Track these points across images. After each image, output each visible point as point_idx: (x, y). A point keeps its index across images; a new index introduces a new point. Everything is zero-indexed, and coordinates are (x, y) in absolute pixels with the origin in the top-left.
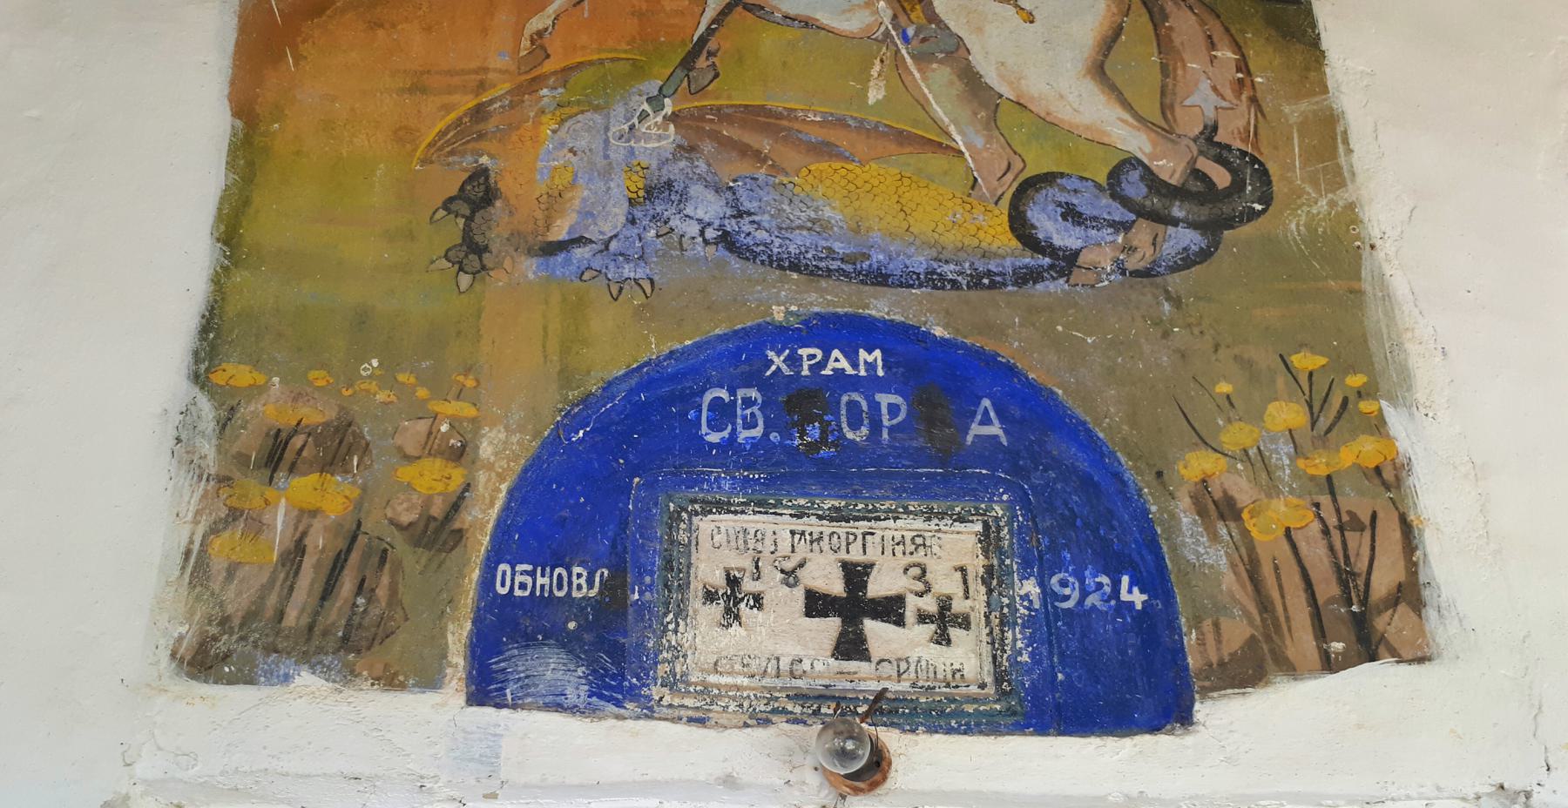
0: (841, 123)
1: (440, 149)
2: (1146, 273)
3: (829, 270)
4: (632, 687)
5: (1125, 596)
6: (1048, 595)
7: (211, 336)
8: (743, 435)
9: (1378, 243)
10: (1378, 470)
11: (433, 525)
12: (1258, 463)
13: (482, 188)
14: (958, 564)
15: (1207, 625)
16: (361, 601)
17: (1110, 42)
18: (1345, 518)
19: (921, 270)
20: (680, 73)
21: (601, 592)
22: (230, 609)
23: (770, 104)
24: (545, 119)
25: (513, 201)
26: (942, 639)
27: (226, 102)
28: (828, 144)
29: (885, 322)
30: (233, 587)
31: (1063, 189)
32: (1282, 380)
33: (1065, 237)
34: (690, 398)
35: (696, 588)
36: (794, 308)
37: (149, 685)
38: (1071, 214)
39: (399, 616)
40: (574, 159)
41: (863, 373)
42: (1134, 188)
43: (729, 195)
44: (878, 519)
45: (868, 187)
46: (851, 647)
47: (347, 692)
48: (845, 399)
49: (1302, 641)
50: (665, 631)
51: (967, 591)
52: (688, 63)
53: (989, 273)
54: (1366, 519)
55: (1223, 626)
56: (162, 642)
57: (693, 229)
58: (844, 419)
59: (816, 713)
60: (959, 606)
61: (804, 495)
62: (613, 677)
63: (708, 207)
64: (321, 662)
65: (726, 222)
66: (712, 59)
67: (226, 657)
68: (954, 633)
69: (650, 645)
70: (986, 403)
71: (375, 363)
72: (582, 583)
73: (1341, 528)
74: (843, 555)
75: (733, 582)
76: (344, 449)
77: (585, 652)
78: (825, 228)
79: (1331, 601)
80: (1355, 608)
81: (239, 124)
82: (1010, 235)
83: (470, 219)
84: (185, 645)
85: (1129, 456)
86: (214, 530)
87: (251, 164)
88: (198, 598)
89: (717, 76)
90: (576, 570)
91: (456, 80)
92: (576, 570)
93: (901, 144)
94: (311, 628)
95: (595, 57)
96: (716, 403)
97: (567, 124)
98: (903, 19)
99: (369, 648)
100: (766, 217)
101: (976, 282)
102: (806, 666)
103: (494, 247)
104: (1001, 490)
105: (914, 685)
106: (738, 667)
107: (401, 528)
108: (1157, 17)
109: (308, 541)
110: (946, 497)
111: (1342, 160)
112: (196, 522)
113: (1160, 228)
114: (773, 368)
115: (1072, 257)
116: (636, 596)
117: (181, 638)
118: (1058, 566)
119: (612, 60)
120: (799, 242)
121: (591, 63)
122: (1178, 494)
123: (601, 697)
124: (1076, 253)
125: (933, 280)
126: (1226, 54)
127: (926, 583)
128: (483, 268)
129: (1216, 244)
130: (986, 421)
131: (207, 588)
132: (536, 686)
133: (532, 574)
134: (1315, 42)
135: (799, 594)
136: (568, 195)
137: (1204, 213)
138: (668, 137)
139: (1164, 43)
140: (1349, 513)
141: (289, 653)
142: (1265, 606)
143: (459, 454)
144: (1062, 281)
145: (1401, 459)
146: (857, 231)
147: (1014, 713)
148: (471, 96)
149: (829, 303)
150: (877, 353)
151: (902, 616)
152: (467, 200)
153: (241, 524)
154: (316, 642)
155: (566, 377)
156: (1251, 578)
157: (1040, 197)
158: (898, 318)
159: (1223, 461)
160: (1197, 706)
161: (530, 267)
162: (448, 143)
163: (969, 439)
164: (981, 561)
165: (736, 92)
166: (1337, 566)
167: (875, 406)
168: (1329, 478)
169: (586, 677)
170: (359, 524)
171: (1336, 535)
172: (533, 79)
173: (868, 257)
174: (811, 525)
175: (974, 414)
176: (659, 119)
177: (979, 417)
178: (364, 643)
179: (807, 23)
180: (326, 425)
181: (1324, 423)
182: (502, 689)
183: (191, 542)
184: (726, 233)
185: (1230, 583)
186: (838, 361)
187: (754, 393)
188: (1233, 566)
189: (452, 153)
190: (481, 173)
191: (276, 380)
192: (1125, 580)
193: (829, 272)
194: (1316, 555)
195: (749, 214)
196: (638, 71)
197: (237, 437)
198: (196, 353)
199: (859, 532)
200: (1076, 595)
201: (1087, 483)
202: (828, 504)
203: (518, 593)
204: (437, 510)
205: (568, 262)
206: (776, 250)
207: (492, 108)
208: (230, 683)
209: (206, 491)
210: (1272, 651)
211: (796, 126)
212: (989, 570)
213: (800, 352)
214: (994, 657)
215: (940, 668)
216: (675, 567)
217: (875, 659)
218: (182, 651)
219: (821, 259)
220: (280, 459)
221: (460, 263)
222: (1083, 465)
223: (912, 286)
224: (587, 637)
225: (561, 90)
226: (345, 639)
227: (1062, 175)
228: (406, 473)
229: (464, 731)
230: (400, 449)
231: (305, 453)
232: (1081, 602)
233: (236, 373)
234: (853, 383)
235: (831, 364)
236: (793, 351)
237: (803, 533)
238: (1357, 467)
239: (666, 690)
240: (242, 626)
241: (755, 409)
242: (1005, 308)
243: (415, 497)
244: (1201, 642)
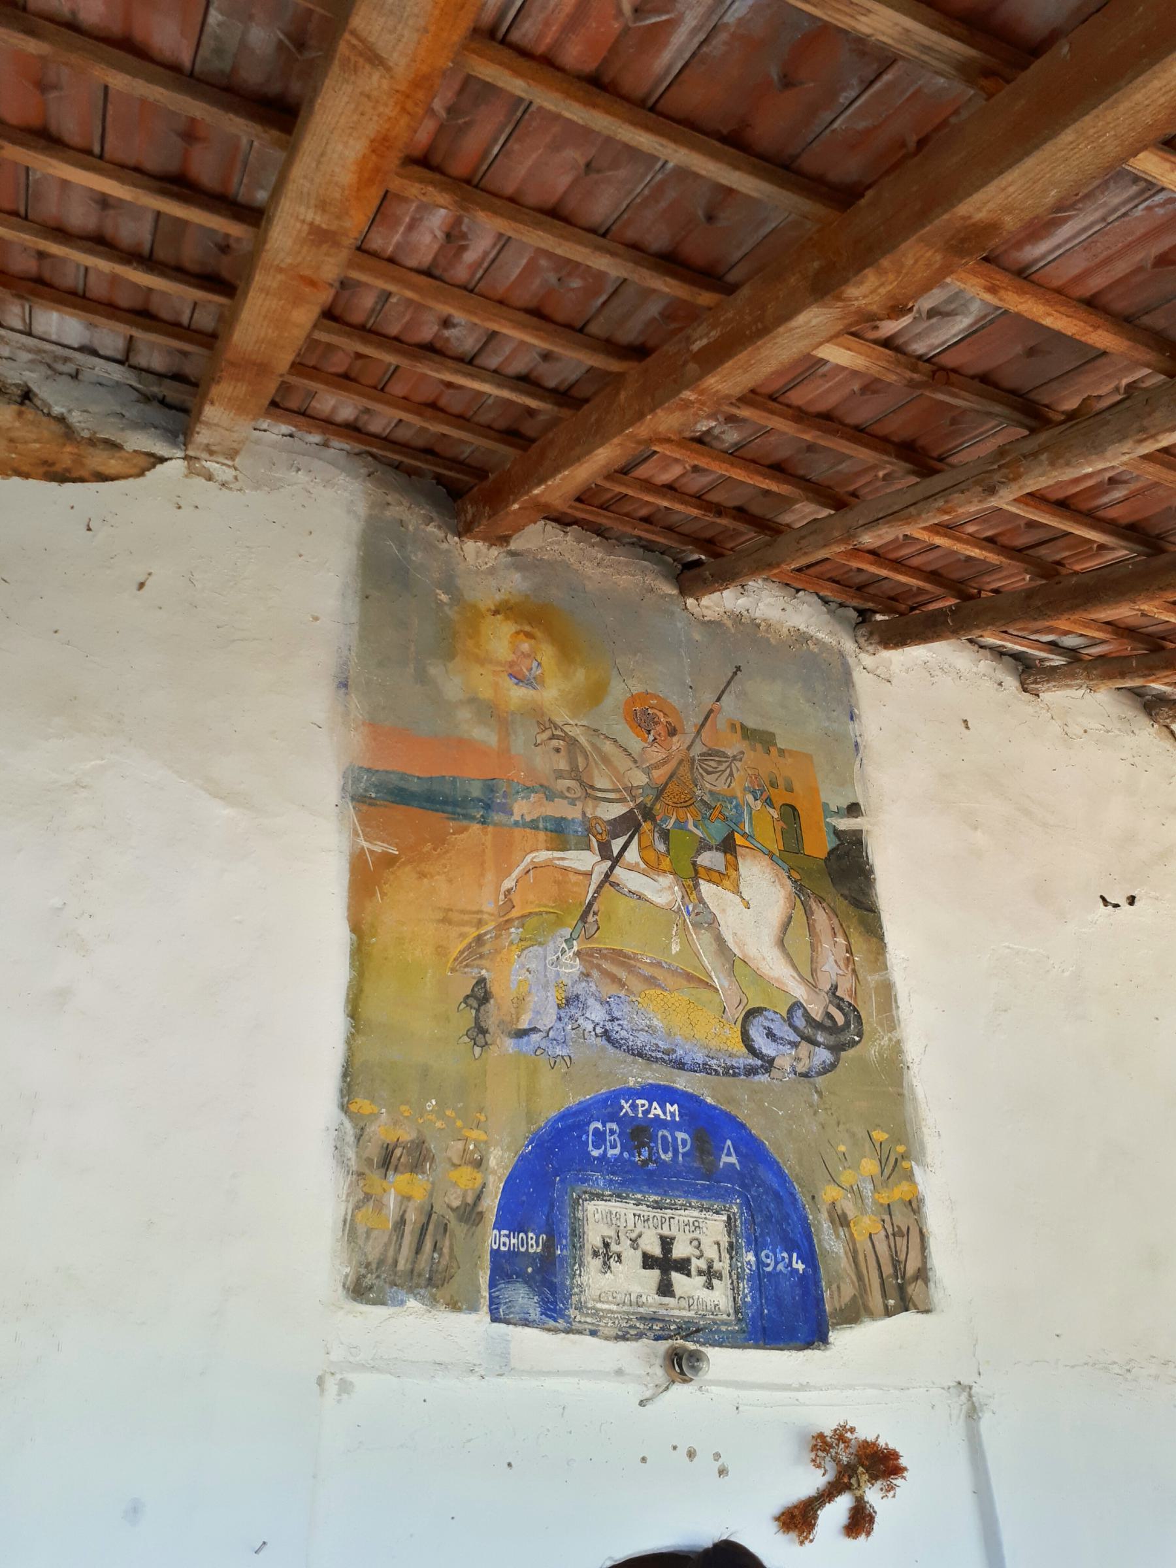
0: (659, 964)
1: (461, 962)
2: (805, 1075)
3: (657, 1058)
4: (561, 1309)
5: (795, 1266)
6: (759, 1262)
7: (348, 1079)
8: (611, 1153)
9: (911, 1065)
10: (910, 1202)
11: (468, 1209)
12: (858, 1195)
13: (483, 990)
14: (715, 1239)
15: (834, 1286)
16: (436, 1255)
17: (786, 925)
18: (896, 1229)
19: (700, 1062)
20: (580, 925)
21: (543, 1249)
22: (370, 1258)
23: (626, 949)
24: (514, 947)
25: (499, 1001)
26: (709, 1286)
27: (347, 922)
28: (654, 978)
29: (682, 1091)
30: (370, 1243)
31: (766, 1018)
32: (868, 1144)
33: (768, 1048)
34: (582, 1127)
35: (588, 1248)
36: (639, 1080)
37: (333, 1304)
38: (770, 1034)
39: (455, 1265)
40: (530, 976)
41: (669, 1118)
42: (800, 1022)
43: (607, 1006)
44: (676, 1209)
45: (674, 1007)
46: (665, 1289)
47: (434, 1312)
48: (660, 1134)
49: (875, 1299)
50: (575, 1275)
51: (720, 1257)
52: (583, 918)
53: (732, 1067)
54: (905, 1230)
55: (842, 1288)
56: (338, 1277)
57: (590, 1027)
58: (660, 1146)
59: (651, 1329)
60: (717, 1266)
61: (640, 1192)
62: (552, 1303)
63: (597, 1013)
64: (419, 1293)
65: (606, 1023)
66: (596, 917)
67: (370, 1288)
68: (715, 1282)
69: (568, 1283)
70: (729, 1142)
71: (434, 1102)
72: (533, 1243)
73: (894, 1235)
74: (659, 1231)
75: (606, 1245)
76: (422, 1158)
77: (537, 1287)
78: (654, 1032)
79: (888, 1277)
80: (899, 1281)
81: (354, 937)
82: (742, 1044)
83: (478, 1010)
84: (349, 1278)
85: (799, 1184)
86: (357, 1207)
87: (362, 965)
88: (353, 1250)
89: (598, 929)
90: (531, 1235)
91: (466, 917)
92: (531, 1235)
93: (689, 981)
94: (412, 1271)
95: (537, 910)
96: (596, 1129)
97: (525, 952)
98: (686, 899)
99: (442, 1285)
100: (625, 1022)
101: (726, 1074)
102: (644, 1299)
103: (491, 1030)
104: (738, 1201)
105: (696, 1313)
106: (610, 1299)
107: (453, 1210)
108: (809, 913)
109: (407, 1216)
110: (710, 1198)
111: (894, 1012)
112: (348, 1201)
113: (812, 1047)
114: (624, 1111)
115: (771, 1061)
116: (559, 1252)
117: (347, 1276)
118: (764, 1247)
119: (547, 913)
120: (641, 1039)
121: (536, 914)
122: (822, 1210)
123: (547, 1316)
124: (773, 1059)
125: (706, 1069)
126: (841, 940)
127: (701, 1251)
128: (486, 1044)
129: (837, 1060)
130: (729, 1154)
131: (356, 1243)
132: (514, 1307)
133: (508, 1236)
134: (881, 938)
135: (639, 1254)
136: (527, 999)
137: (832, 1040)
138: (575, 967)
139: (811, 927)
140: (898, 1226)
141: (402, 1287)
142: (860, 1278)
143: (479, 1164)
144: (767, 1075)
145: (920, 1196)
146: (669, 1034)
147: (744, 1332)
148: (474, 929)
149: (657, 1078)
150: (676, 1106)
151: (689, 1271)
152: (476, 998)
153: (371, 1203)
154: (415, 1280)
155: (530, 1117)
156: (854, 1262)
157: (755, 1022)
158: (690, 1090)
159: (842, 1191)
160: (830, 1334)
161: (509, 1045)
162: (465, 959)
163: (721, 1164)
164: (726, 1239)
165: (608, 941)
166: (892, 1256)
167: (675, 1139)
168: (889, 1205)
169: (538, 1303)
170: (432, 1207)
171: (891, 1237)
172: (507, 921)
173: (675, 1052)
174: (644, 1210)
175: (723, 1148)
176: (571, 954)
177: (725, 1151)
178: (440, 1282)
179: (640, 897)
180: (412, 1142)
181: (887, 1172)
182: (497, 1309)
183: (346, 1214)
184: (606, 1031)
185: (845, 1263)
186: (656, 1110)
187: (614, 1126)
188: (846, 1253)
189: (467, 966)
190: (482, 981)
191: (384, 1110)
192: (795, 1255)
193: (657, 1060)
194: (882, 1248)
195: (618, 1020)
196: (559, 922)
197: (366, 1147)
198: (341, 1091)
199: (667, 1217)
200: (773, 1264)
201: (777, 1195)
202: (653, 1198)
203: (502, 1248)
204: (470, 1200)
205: (528, 1044)
206: (631, 1043)
207: (486, 938)
208: (374, 1304)
209: (351, 1181)
210: (863, 1304)
211: (638, 965)
212: (731, 1244)
213: (637, 1101)
214: (734, 1298)
215: (708, 1305)
216: (577, 1233)
217: (677, 1297)
218: (348, 1283)
219: (653, 1051)
220: (390, 1162)
221: (474, 1039)
222: (776, 1186)
223: (696, 1071)
224: (538, 1277)
225: (521, 930)
226: (430, 1279)
227: (766, 1009)
228: (454, 1175)
229: (492, 1338)
230: (450, 1159)
231: (402, 1160)
232: (775, 1268)
233: (363, 1105)
234: (662, 1124)
235: (653, 1111)
236: (634, 1101)
237: (639, 1216)
238: (902, 1200)
239: (577, 1312)
240: (377, 1269)
241: (615, 1136)
242: (740, 1088)
243: (459, 1190)
244: (832, 1298)
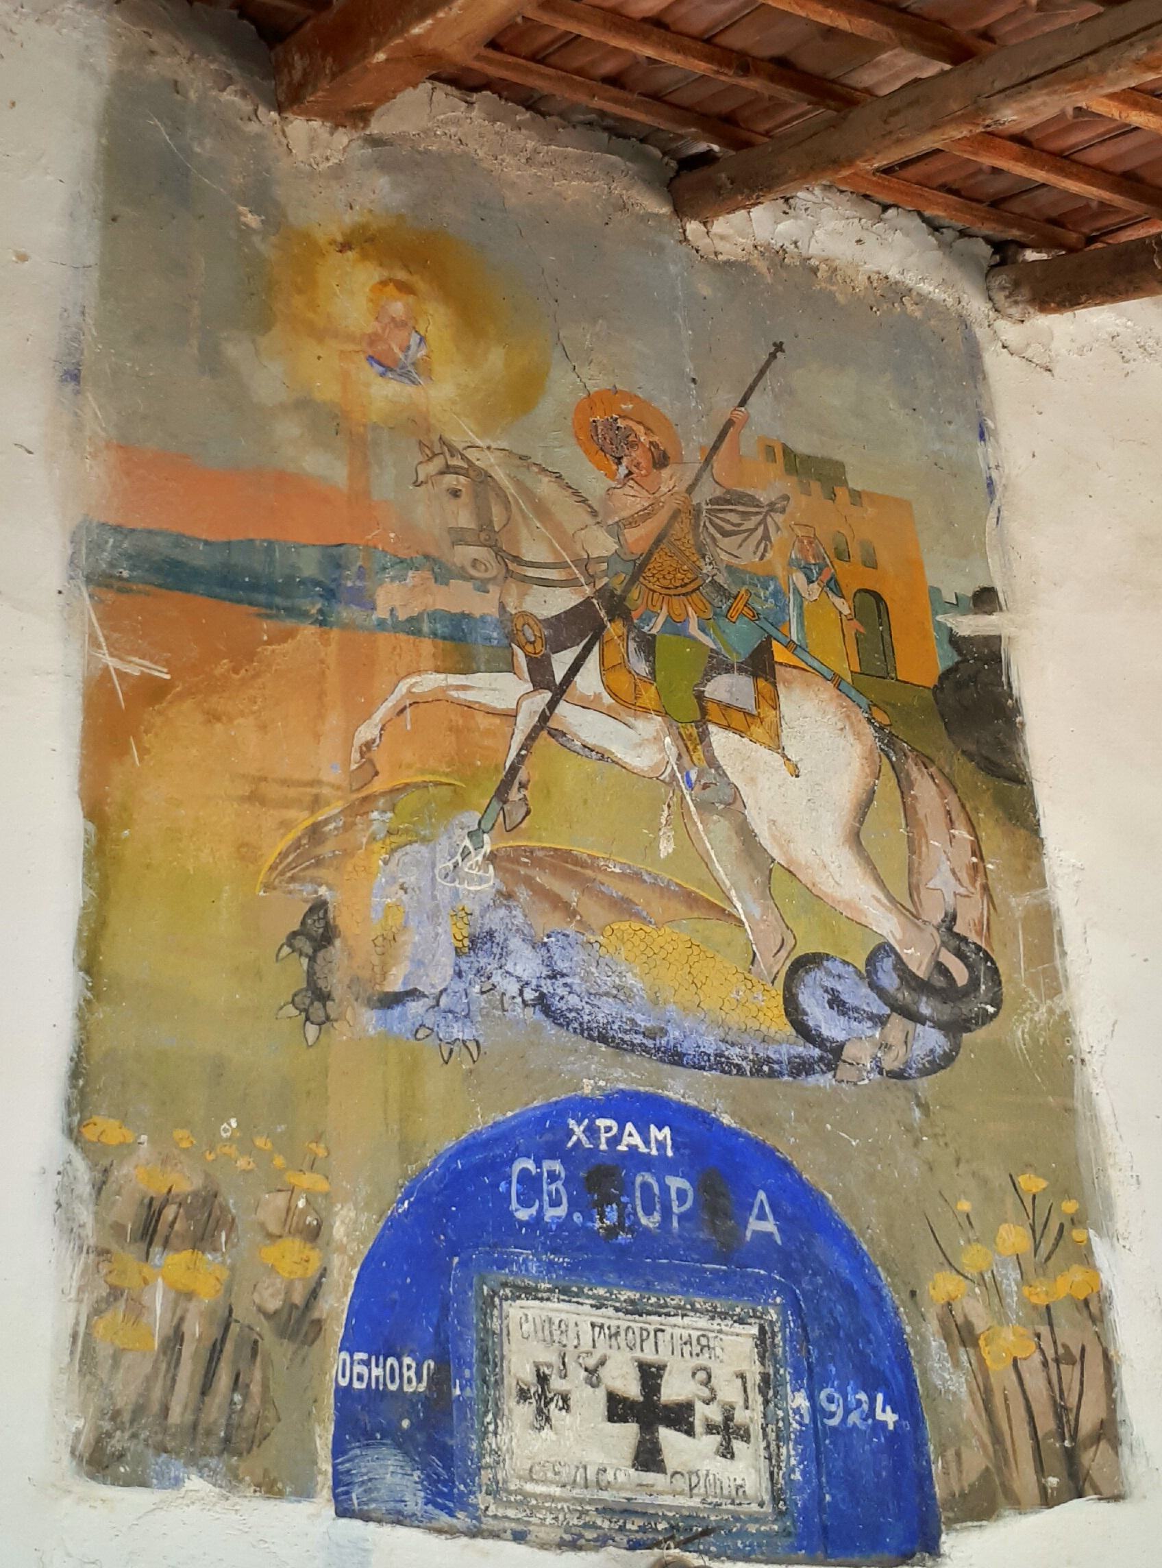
0: (636, 877)
1: (282, 873)
2: (899, 1075)
3: (633, 1044)
4: (461, 1493)
5: (880, 1416)
6: (815, 1409)
7: (81, 1082)
8: (551, 1214)
9: (1087, 1057)
10: (1086, 1302)
11: (295, 1314)
12: (991, 1287)
13: (322, 923)
15: (950, 1453)
16: (237, 1398)
17: (864, 806)
18: (1061, 1351)
19: (710, 1051)
20: (496, 805)
21: (429, 1387)
22: (120, 1403)
23: (580, 850)
24: (377, 846)
26: (727, 1452)
27: (78, 801)
29: (678, 1103)
31: (829, 973)
32: (1010, 1199)
33: (832, 1027)
34: (499, 1168)
35: (510, 1383)
36: (602, 1083)
37: (54, 1485)
38: (836, 1002)
39: (271, 1414)
40: (405, 897)
41: (654, 1152)
42: (890, 981)
43: (543, 951)
44: (668, 1315)
45: (663, 954)
47: (234, 1499)
48: (639, 1180)
49: (1024, 1476)
50: (486, 1433)
51: (746, 1400)
52: (501, 793)
53: (768, 1061)
54: (1076, 1352)
55: (964, 1456)
56: (62, 1437)
57: (513, 988)
58: (638, 1202)
59: (622, 1529)
60: (740, 1416)
61: (604, 1284)
62: (445, 1483)
64: (206, 1466)
65: (543, 982)
66: (523, 792)
67: (120, 1457)
68: (737, 1445)
69: (474, 1447)
70: (762, 1195)
71: (234, 1123)
73: (1057, 1361)
74: (638, 1354)
75: (543, 1379)
77: (419, 1454)
79: (1047, 1436)
80: (1067, 1443)
81: (91, 827)
82: (785, 1020)
83: (312, 959)
84: (83, 1439)
85: (888, 1271)
86: (97, 1312)
87: (105, 877)
88: (89, 1389)
89: (528, 813)
90: (407, 1360)
91: (292, 792)
92: (407, 1360)
94: (195, 1426)
95: (419, 779)
96: (524, 1171)
97: (397, 855)
98: (686, 758)
99: (249, 1451)
100: (577, 980)
101: (757, 1072)
102: (609, 1476)
103: (335, 995)
104: (778, 1300)
105: (704, 1501)
106: (550, 1475)
107: (269, 1316)
108: (904, 785)
109: (186, 1327)
110: (728, 1294)
111: (1058, 962)
112: (80, 1301)
113: (910, 1025)
114: (574, 1138)
115: (838, 1049)
116: (457, 1392)
117: (78, 1434)
118: (825, 1382)
119: (438, 784)
120: (605, 1011)
121: (417, 786)
122: (928, 1316)
125: (721, 1064)
126: (962, 833)
127: (712, 1390)
128: (328, 1018)
129: (956, 1048)
130: (762, 1217)
131: (94, 1375)
132: (378, 1490)
133: (367, 1363)
135: (601, 1395)
137: (946, 1012)
138: (487, 881)
139: (909, 811)
140: (1064, 1346)
141: (177, 1454)
142: (997, 1437)
143: (314, 1234)
144: (830, 1075)
145: (1104, 1292)
146: (655, 1002)
149: (633, 1081)
150: (667, 1130)
151: (691, 1425)
152: (310, 938)
153: (122, 1304)
154: (201, 1442)
155: (406, 1150)
156: (986, 1409)
157: (809, 979)
158: (692, 1102)
160: (943, 1538)
161: (369, 1020)
162: (289, 867)
163: (748, 1234)
166: (1055, 1401)
167: (665, 1189)
168: (1048, 1308)
169: (421, 1483)
171: (1052, 1365)
172: (365, 799)
173: (664, 1032)
174: (609, 1317)
175: (752, 1206)
176: (480, 858)
177: (755, 1211)
178: (244, 1445)
180: (195, 1194)
181: (1045, 1249)
182: (347, 1493)
183: (77, 1324)
185: (969, 1412)
186: (632, 1138)
187: (557, 1166)
188: (971, 1393)
189: (293, 879)
190: (319, 907)
191: (144, 1138)
192: (880, 1397)
194: (1036, 1384)
195: (563, 975)
196: (458, 801)
197: (114, 1203)
199: (651, 1328)
200: (840, 1413)
201: (848, 1291)
202: (626, 1294)
203: (357, 1385)
204: (298, 1298)
205: (402, 1018)
206: (586, 1018)
207: (327, 829)
208: (127, 1484)
209: (86, 1264)
210: (1003, 1484)
211: (600, 877)
212: (765, 1378)
214: (772, 1474)
215: (725, 1485)
216: (490, 1358)
217: (670, 1471)
218: (80, 1447)
219: (626, 1032)
220: (155, 1231)
221: (306, 1011)
222: (846, 1273)
223: (703, 1068)
224: (420, 1437)
225: (390, 815)
226: (227, 1440)
227: (827, 957)
228: (270, 1253)
229: (338, 1545)
230: (262, 1226)
231: (177, 1226)
233: (107, 1129)
235: (626, 1140)
236: (592, 1122)
237: (602, 1327)
238: (1071, 1298)
239: (490, 1498)
240: (132, 1422)
241: (559, 1184)
243: (278, 1281)
244: (946, 1472)
